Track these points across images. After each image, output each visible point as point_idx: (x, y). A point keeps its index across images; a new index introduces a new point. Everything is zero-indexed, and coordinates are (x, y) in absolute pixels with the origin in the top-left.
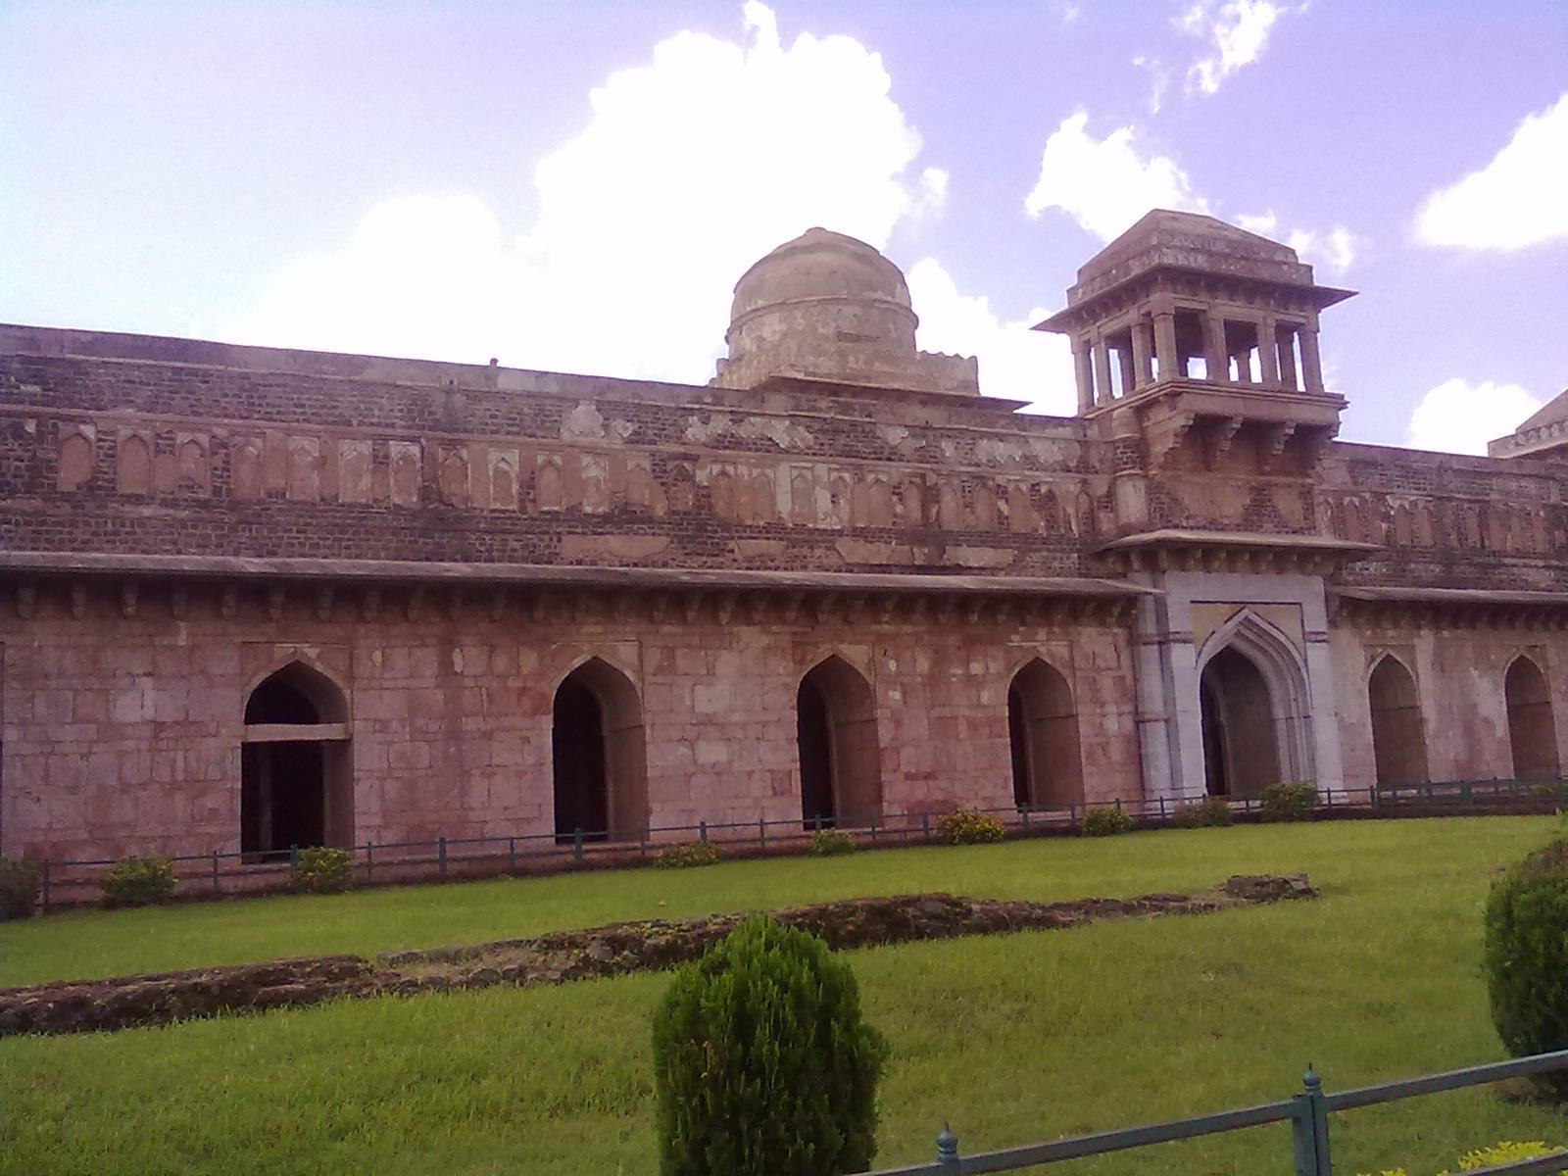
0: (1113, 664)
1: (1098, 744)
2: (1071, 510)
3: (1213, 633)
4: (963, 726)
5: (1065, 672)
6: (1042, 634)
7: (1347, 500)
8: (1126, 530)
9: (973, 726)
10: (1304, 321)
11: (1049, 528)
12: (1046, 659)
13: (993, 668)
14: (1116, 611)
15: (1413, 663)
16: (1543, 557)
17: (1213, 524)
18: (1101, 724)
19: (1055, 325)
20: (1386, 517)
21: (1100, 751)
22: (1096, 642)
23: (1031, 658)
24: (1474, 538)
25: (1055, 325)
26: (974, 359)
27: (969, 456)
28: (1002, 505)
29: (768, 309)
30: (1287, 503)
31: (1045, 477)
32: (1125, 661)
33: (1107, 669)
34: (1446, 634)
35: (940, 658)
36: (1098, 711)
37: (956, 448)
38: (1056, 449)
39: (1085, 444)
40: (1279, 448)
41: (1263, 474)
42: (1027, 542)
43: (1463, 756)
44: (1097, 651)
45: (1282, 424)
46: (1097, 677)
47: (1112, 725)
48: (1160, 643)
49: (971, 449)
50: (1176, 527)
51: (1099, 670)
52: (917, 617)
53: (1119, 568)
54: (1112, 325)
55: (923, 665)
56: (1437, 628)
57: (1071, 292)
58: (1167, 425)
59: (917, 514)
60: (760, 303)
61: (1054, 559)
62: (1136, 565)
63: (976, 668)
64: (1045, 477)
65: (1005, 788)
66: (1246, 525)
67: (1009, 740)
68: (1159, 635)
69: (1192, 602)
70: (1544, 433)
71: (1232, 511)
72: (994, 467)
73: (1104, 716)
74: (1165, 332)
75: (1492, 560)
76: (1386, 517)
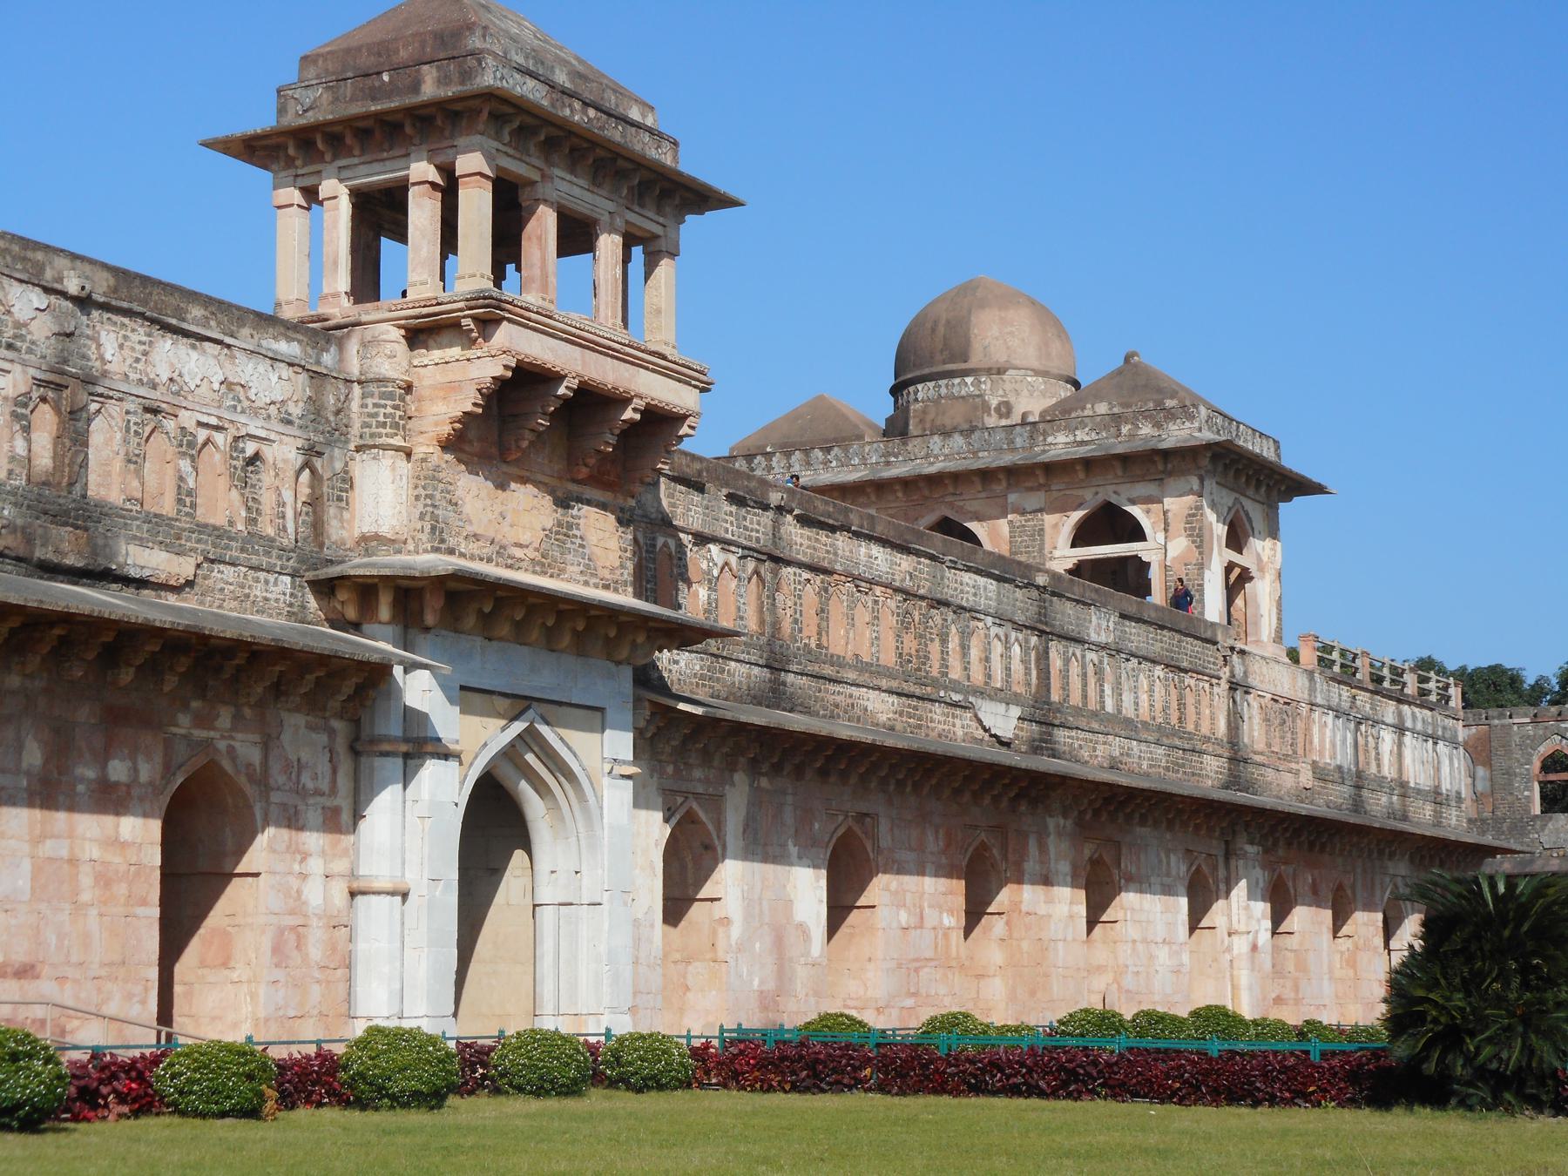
0: (324, 785)
1: (293, 929)
2: (288, 496)
3: (485, 745)
4: (86, 880)
5: (250, 790)
6: (225, 718)
7: (660, 541)
8: (369, 542)
9: (104, 880)
10: (657, 230)
11: (252, 521)
12: (226, 765)
13: (146, 772)
14: (348, 688)
15: (719, 825)
16: (890, 674)
18: (299, 892)
21: (291, 938)
22: (304, 741)
23: (200, 761)
24: (810, 629)
27: (139, 366)
28: (185, 465)
32: (344, 783)
33: (318, 793)
34: (764, 782)
35: (61, 749)
36: (296, 867)
37: (121, 346)
38: (274, 379)
40: (607, 443)
41: (574, 481)
42: (218, 546)
43: (771, 985)
44: (304, 760)
45: (623, 401)
46: (301, 807)
47: (314, 894)
48: (407, 756)
49: (145, 354)
50: (451, 552)
51: (301, 792)
52: (34, 661)
53: (351, 613)
55: (33, 756)
56: (754, 768)
59: (44, 459)
61: (257, 580)
62: (385, 612)
63: (118, 770)
65: (143, 1002)
66: (541, 567)
67: (156, 912)
68: (406, 740)
69: (462, 688)
71: (525, 538)
72: (177, 394)
73: (304, 876)
75: (828, 671)
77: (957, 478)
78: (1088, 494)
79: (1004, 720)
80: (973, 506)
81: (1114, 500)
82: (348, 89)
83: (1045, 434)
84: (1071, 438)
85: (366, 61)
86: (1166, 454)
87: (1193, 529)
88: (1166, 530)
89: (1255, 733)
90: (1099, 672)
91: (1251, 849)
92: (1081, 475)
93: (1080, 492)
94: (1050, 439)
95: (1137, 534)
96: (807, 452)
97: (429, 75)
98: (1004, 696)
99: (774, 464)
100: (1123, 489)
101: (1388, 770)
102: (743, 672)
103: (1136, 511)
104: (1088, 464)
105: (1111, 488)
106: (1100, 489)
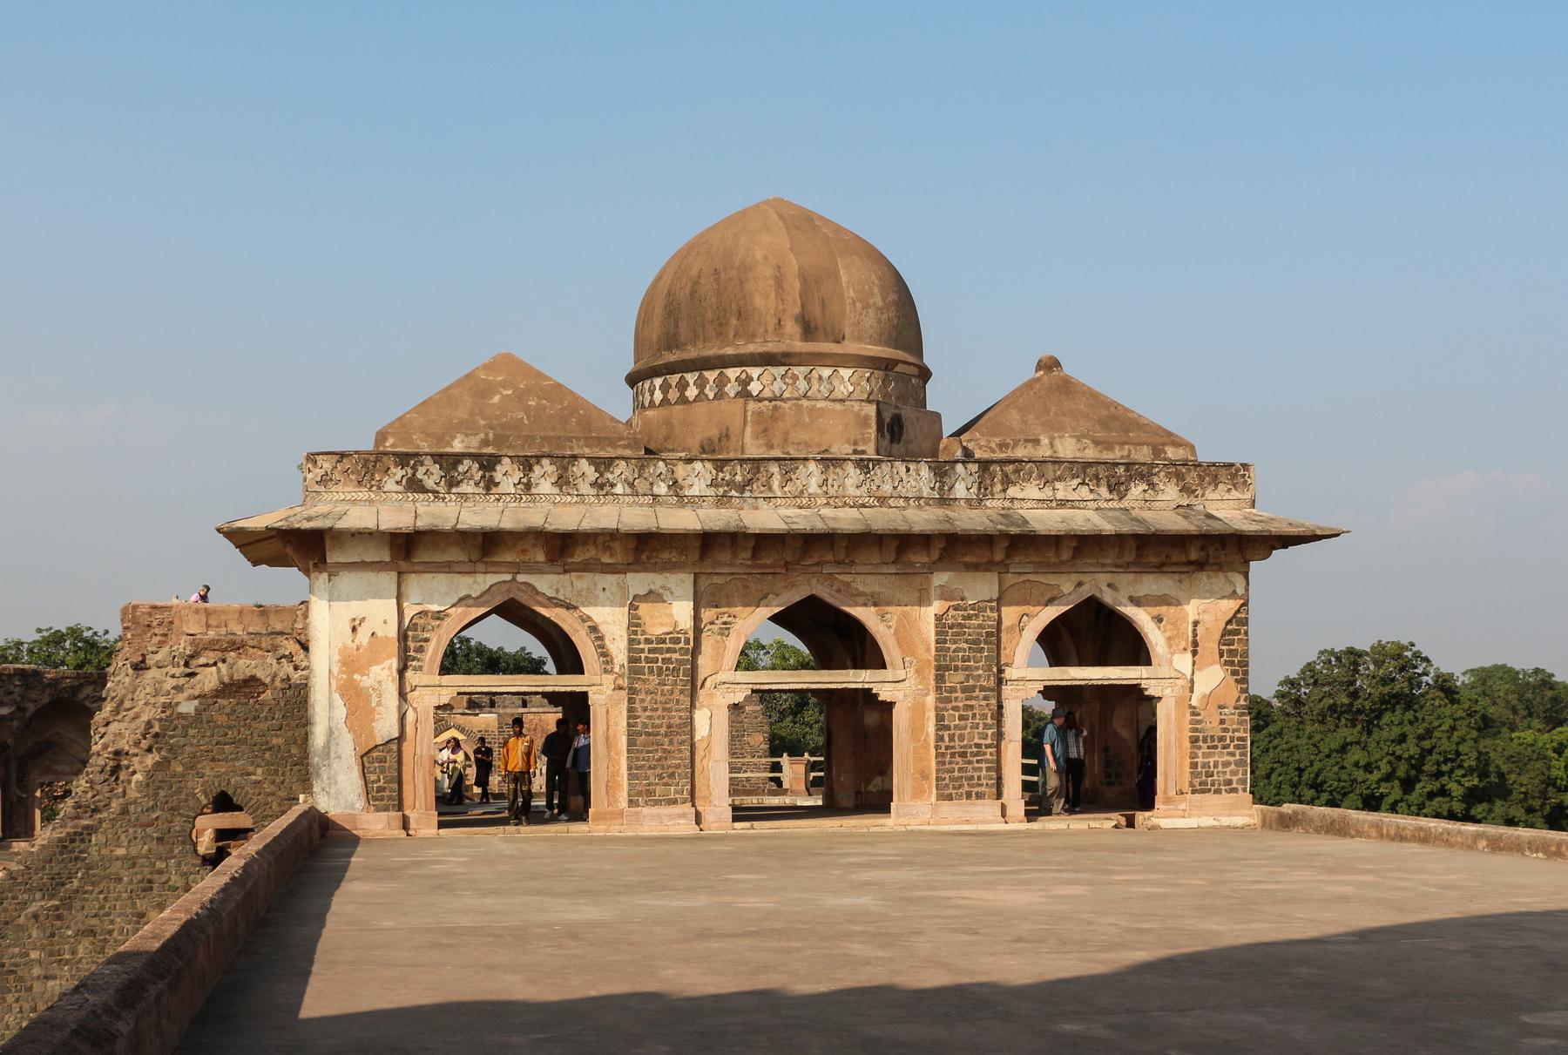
70: (508, 476)
78: (1066, 584)
80: (866, 584)
81: (1108, 597)
83: (1007, 482)
84: (1047, 493)
87: (1232, 653)
88: (1195, 653)
92: (1066, 555)
93: (1052, 580)
94: (1013, 491)
95: (1138, 652)
96: (565, 462)
99: (498, 476)
100: (1123, 579)
103: (1141, 617)
105: (1103, 579)
106: (1086, 578)
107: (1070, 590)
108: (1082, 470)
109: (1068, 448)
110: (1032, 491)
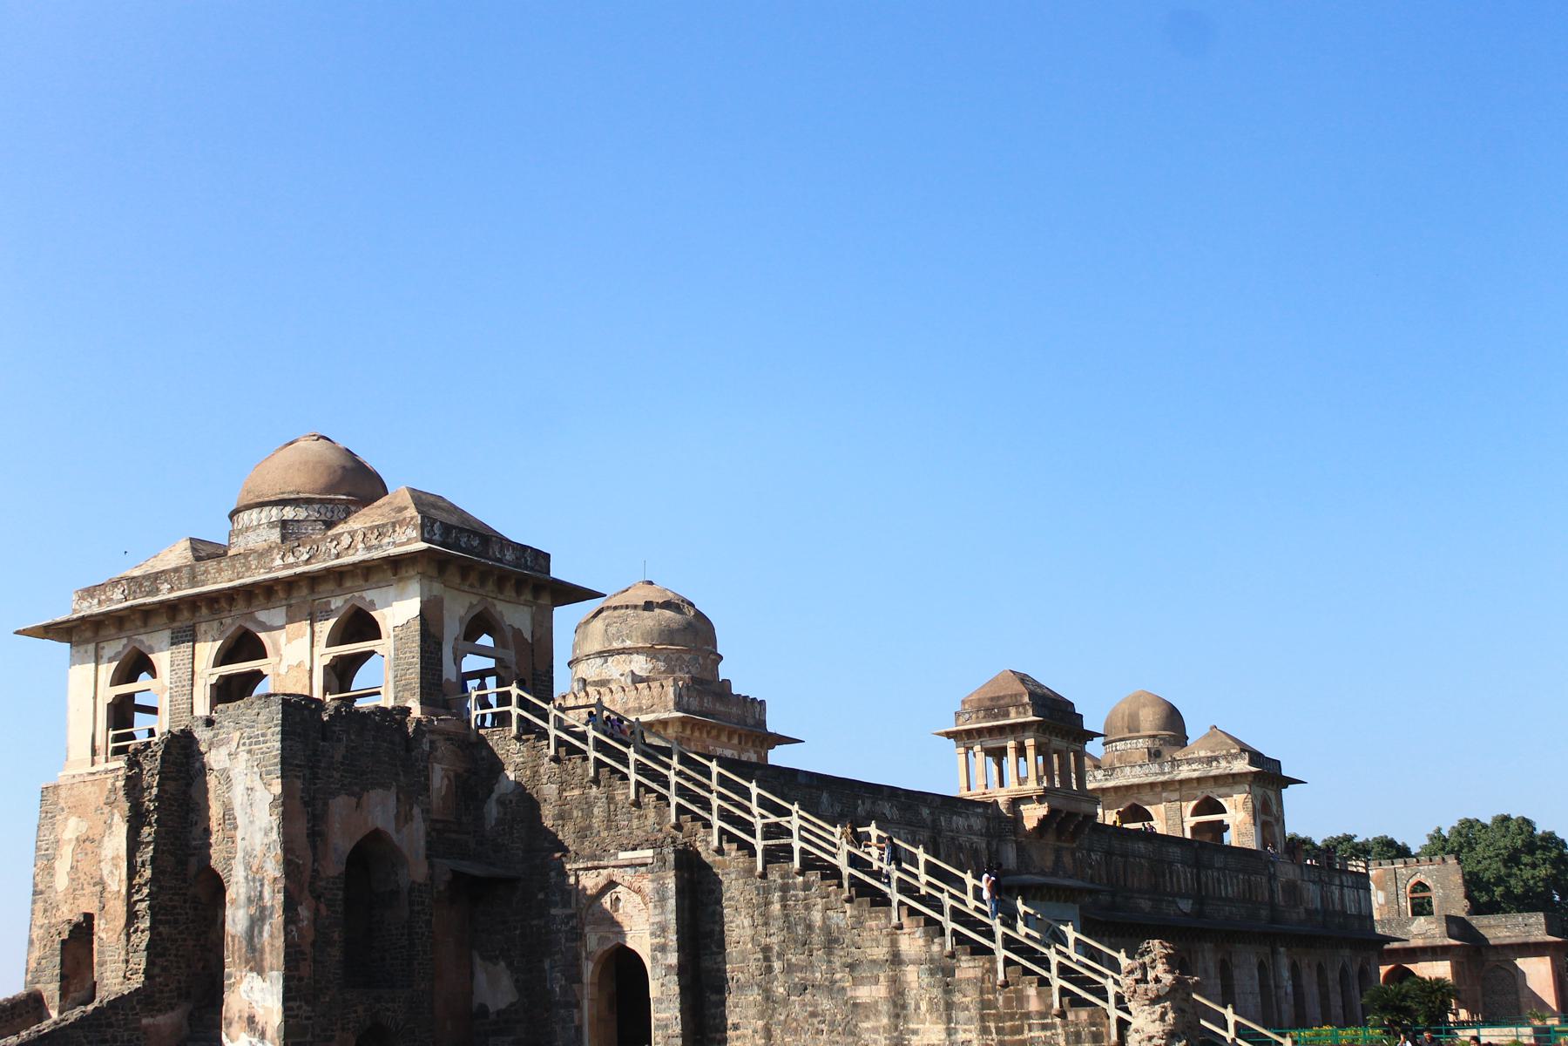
17: (1042, 873)
19: (949, 735)
20: (1091, 866)
25: (949, 735)
26: (762, 703)
29: (637, 651)
30: (1067, 859)
31: (975, 839)
39: (988, 819)
45: (1077, 815)
54: (992, 743)
57: (958, 715)
58: (1033, 815)
60: (628, 644)
64: (975, 839)
66: (1054, 874)
74: (1031, 753)
76: (1091, 866)
77: (1139, 786)
79: (1186, 906)
80: (1146, 798)
82: (982, 714)
85: (988, 703)
86: (1234, 775)
89: (1280, 897)
90: (1219, 881)
91: (1282, 950)
95: (1223, 811)
97: (1013, 711)
98: (1183, 896)
101: (1338, 907)
102: (1104, 899)
103: (1221, 800)
104: (1199, 780)
107: (1201, 794)
108: (1200, 760)
109: (1202, 754)
110: (1185, 768)
